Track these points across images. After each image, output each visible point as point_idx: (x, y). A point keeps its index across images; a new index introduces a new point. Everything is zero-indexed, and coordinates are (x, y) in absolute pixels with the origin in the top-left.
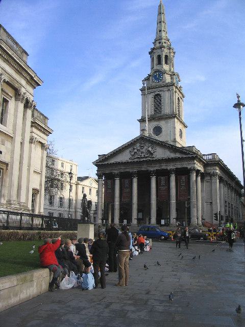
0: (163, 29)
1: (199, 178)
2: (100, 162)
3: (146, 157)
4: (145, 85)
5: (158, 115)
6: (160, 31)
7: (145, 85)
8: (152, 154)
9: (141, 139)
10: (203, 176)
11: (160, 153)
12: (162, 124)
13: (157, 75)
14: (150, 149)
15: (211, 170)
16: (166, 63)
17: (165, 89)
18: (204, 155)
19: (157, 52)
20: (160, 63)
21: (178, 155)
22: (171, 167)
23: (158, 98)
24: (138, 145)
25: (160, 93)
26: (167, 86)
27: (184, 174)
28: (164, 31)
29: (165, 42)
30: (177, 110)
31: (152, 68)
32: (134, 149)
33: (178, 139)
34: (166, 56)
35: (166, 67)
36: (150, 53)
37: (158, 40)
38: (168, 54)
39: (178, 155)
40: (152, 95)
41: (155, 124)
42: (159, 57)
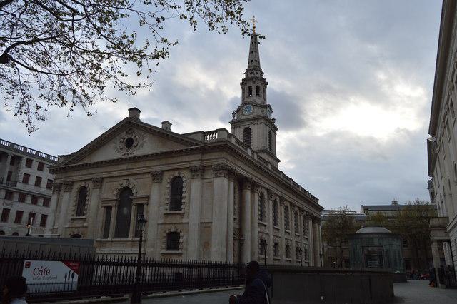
4: (236, 118)
7: (236, 118)
16: (258, 93)
20: (250, 92)
28: (256, 61)
34: (258, 88)
36: (241, 84)
38: (260, 85)
40: (242, 129)
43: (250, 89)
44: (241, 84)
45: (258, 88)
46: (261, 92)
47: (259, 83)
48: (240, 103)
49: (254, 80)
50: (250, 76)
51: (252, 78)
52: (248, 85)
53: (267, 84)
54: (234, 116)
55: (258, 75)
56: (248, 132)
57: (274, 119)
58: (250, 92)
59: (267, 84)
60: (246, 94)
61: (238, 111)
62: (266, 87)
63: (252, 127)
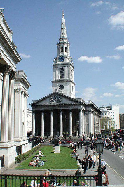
2: (34, 104)
3: (58, 103)
8: (61, 101)
10: (85, 111)
11: (64, 101)
14: (60, 99)
15: (88, 109)
16: (66, 51)
17: (66, 66)
20: (62, 51)
21: (73, 103)
22: (70, 108)
25: (63, 68)
26: (67, 64)
34: (66, 48)
38: (67, 46)
39: (73, 103)
41: (61, 84)
42: (62, 48)
45: (66, 48)
58: (62, 51)
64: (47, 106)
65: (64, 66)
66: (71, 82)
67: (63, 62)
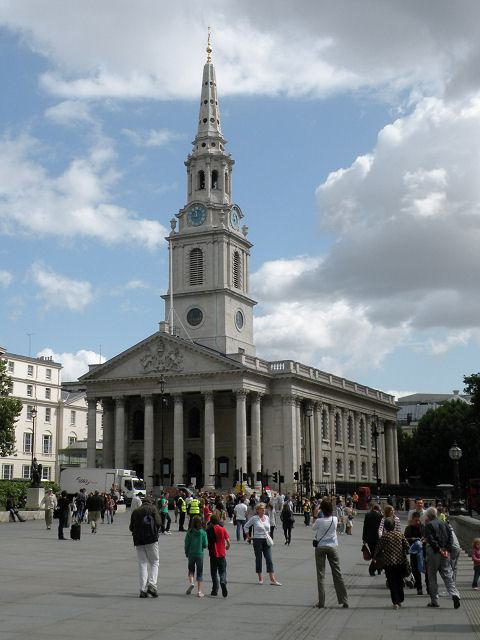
0: (211, 116)
1: (257, 407)
5: (194, 288)
6: (205, 121)
7: (177, 230)
9: (159, 340)
12: (203, 305)
13: (194, 211)
14: (173, 357)
15: (280, 390)
17: (209, 239)
18: (274, 363)
19: (200, 165)
20: (202, 186)
23: (196, 253)
24: (154, 349)
26: (213, 234)
27: (226, 401)
29: (213, 145)
30: (232, 280)
31: (190, 195)
32: (147, 356)
33: (230, 328)
35: (212, 197)
37: (201, 141)
43: (202, 175)
44: (186, 164)
46: (222, 179)
47: (214, 166)
48: (182, 202)
49: (208, 160)
50: (202, 150)
51: (207, 156)
52: (199, 169)
53: (231, 163)
54: (173, 227)
55: (212, 151)
56: (196, 252)
57: (245, 229)
59: (231, 163)
60: (196, 183)
61: (179, 216)
62: (230, 170)
63: (204, 247)
64: (132, 381)
65: (202, 239)
66: (227, 298)
67: (201, 228)
